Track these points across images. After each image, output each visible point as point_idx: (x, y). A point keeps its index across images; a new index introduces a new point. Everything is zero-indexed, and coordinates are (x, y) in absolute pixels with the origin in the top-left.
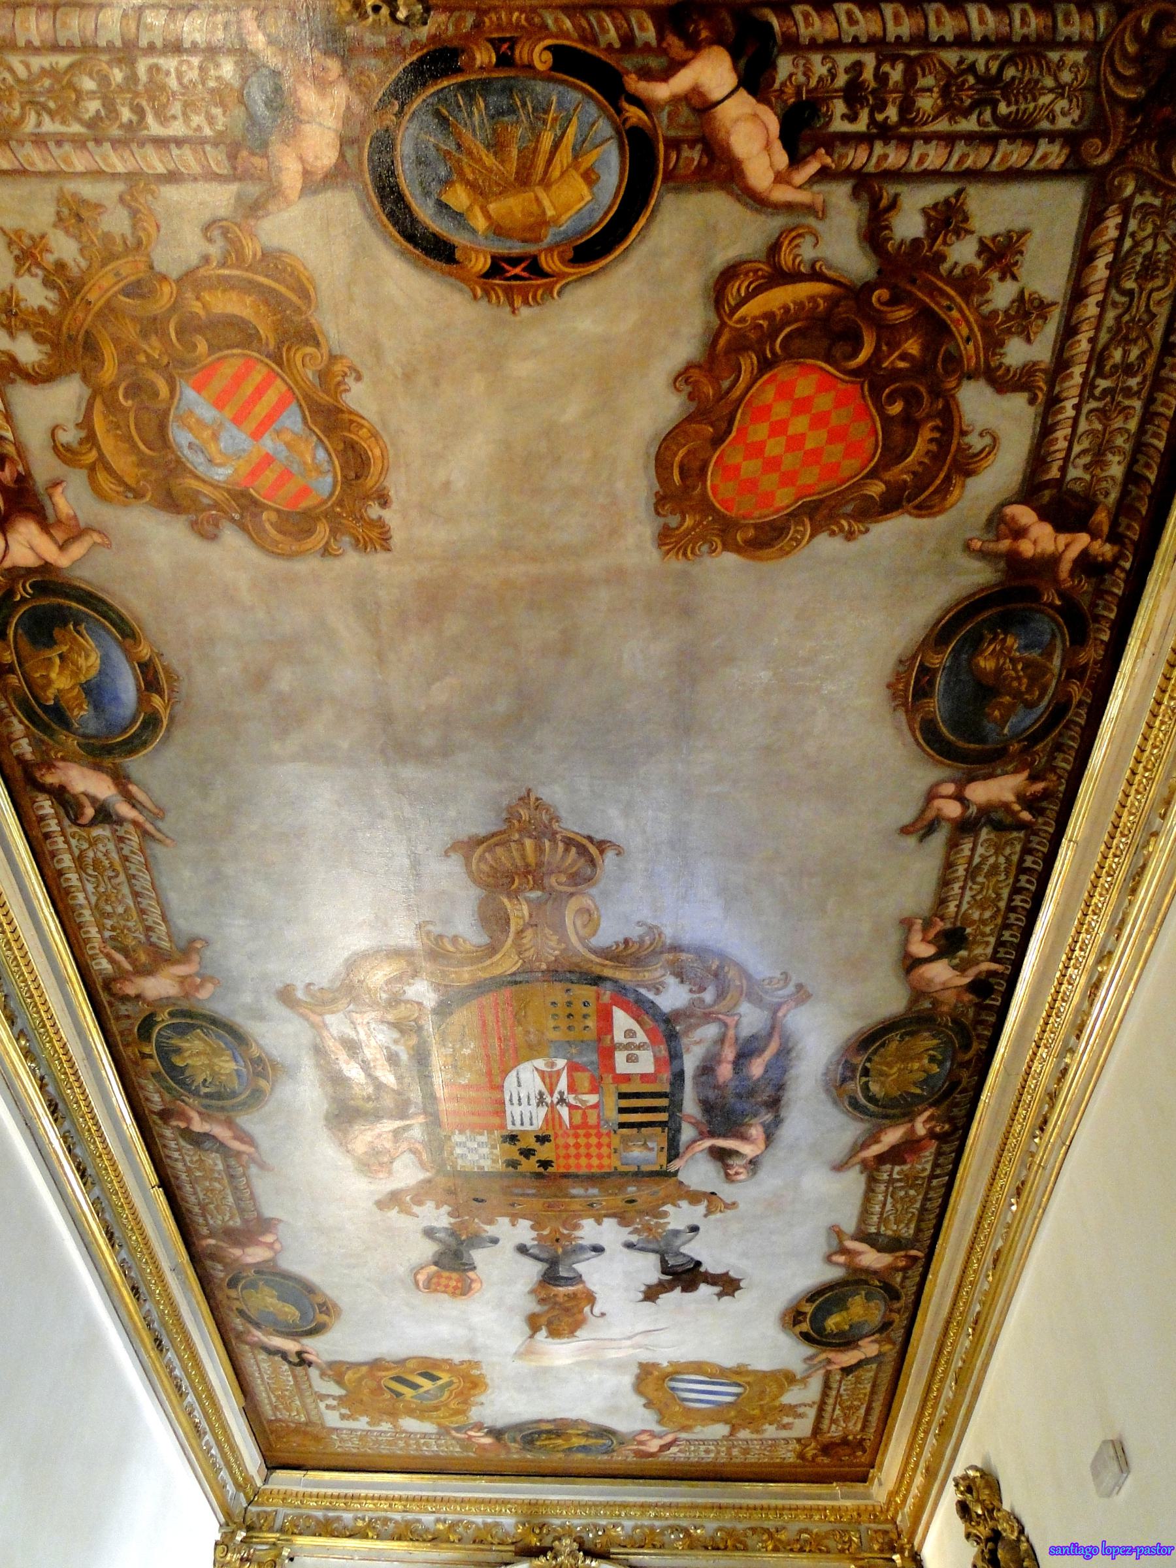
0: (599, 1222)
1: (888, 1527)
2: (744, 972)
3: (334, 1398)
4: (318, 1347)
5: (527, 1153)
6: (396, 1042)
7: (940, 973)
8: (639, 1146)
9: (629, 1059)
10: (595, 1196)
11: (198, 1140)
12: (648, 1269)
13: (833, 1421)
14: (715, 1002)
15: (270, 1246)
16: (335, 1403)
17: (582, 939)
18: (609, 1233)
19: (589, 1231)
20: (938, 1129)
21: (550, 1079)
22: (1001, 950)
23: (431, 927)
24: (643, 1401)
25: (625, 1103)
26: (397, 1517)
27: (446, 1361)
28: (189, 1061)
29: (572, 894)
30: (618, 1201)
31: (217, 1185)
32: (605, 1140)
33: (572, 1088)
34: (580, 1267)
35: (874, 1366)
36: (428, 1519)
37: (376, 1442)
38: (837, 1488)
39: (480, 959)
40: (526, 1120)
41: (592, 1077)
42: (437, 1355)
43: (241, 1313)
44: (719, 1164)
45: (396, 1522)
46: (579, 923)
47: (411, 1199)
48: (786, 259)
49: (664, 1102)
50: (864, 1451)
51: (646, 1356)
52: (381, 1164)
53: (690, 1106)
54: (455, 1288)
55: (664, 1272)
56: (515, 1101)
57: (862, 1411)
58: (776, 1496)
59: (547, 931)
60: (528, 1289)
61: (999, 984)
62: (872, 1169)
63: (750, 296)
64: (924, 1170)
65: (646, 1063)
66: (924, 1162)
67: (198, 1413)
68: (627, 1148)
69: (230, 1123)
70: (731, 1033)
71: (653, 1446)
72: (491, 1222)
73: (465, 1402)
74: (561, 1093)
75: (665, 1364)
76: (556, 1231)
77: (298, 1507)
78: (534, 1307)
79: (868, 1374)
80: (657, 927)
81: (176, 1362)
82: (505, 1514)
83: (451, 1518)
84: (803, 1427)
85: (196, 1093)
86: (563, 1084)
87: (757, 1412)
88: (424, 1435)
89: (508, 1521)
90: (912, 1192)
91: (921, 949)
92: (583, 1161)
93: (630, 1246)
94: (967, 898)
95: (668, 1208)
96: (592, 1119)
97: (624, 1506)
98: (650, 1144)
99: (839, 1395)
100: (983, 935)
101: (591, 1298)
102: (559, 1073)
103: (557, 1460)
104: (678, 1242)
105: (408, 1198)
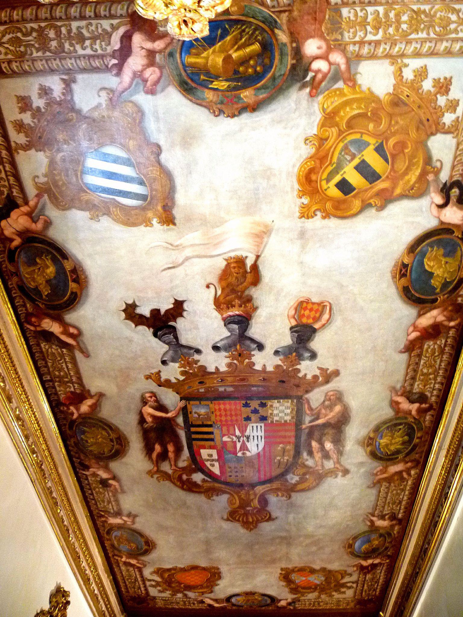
5: (255, 411)
9: (211, 455)
10: (221, 386)
21: (244, 448)
25: (211, 436)
30: (209, 383)
32: (218, 418)
40: (255, 428)
44: (161, 403)
46: (234, 501)
47: (319, 378)
49: (194, 436)
53: (182, 434)
55: (174, 329)
60: (259, 312)
68: (207, 414)
70: (173, 463)
74: (239, 441)
78: (255, 292)
86: (239, 445)
92: (228, 407)
93: (198, 351)
95: (182, 378)
96: (225, 428)
98: (196, 415)
101: (218, 304)
102: (240, 450)
105: (321, 379)
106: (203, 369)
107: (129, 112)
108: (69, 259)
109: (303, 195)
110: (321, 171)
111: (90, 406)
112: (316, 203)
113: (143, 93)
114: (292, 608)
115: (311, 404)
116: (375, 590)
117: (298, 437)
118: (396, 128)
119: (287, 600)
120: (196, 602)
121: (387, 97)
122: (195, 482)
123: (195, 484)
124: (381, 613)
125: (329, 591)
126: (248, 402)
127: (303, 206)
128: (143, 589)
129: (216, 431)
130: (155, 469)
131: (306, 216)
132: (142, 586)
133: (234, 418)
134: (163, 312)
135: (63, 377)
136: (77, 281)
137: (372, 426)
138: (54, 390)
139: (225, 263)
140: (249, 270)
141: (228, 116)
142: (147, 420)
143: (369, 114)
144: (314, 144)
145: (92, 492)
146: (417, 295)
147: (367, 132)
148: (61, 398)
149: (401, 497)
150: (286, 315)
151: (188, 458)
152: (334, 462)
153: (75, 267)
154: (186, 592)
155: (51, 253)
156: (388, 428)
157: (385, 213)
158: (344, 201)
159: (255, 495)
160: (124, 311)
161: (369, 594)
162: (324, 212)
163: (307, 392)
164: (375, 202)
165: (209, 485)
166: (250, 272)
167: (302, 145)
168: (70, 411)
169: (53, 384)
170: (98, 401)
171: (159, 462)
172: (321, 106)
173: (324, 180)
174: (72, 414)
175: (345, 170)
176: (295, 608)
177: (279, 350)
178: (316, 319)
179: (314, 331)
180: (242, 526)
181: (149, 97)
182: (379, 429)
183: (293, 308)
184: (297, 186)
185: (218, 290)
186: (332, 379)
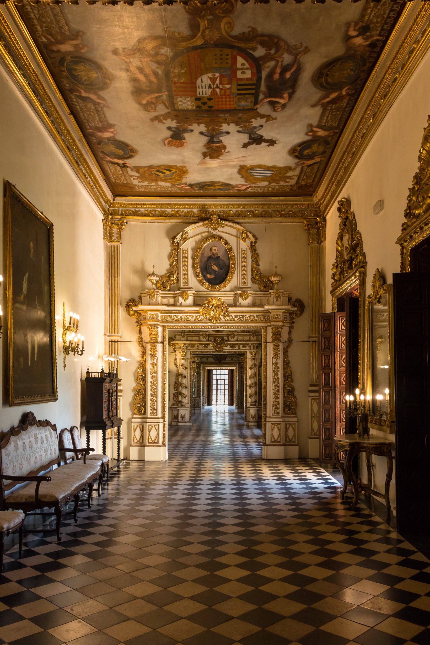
0: (229, 125)
1: (317, 209)
2: (286, 43)
3: (136, 176)
4: (130, 162)
5: (204, 104)
6: (157, 68)
7: (359, 41)
10: (228, 117)
11: (84, 99)
12: (245, 138)
13: (303, 180)
14: (275, 54)
15: (112, 132)
16: (136, 178)
17: (227, 33)
18: (232, 128)
19: (225, 127)
20: (350, 92)
21: (213, 80)
22: (383, 32)
23: (170, 29)
24: (241, 176)
26: (159, 210)
27: (175, 166)
28: (79, 73)
29: (224, 17)
31: (92, 113)
33: (221, 83)
34: (221, 138)
35: (318, 164)
36: (169, 210)
37: (151, 188)
38: (302, 198)
39: (189, 40)
40: (204, 93)
42: (171, 164)
43: (103, 152)
44: (272, 106)
45: (159, 211)
46: (226, 27)
49: (254, 87)
50: (312, 188)
51: (242, 164)
52: (152, 108)
53: (263, 88)
54: (178, 145)
56: (200, 87)
57: (313, 177)
58: (282, 201)
59: (214, 30)
60: (203, 145)
61: (380, 44)
62: (324, 107)
64: (343, 105)
65: (248, 74)
66: (344, 103)
67: (91, 183)
69: (96, 94)
70: (280, 64)
71: (243, 188)
72: (191, 125)
73: (181, 177)
74: (217, 85)
75: (249, 166)
77: (126, 207)
79: (316, 167)
80: (255, 28)
81: (83, 169)
82: (194, 208)
83: (176, 210)
84: (293, 182)
85: (83, 84)
86: (218, 82)
87: (278, 178)
88: (167, 186)
89: (195, 210)
90: (338, 113)
91: (352, 33)
93: (238, 132)
94: (373, 14)
95: (253, 120)
96: (228, 93)
97: (232, 205)
98: (248, 100)
99: (306, 173)
100: (377, 27)
101: (225, 147)
102: (216, 78)
103: (211, 192)
104: (256, 130)
105: (162, 118)
122: (263, 47)
126: (209, 109)
129: (235, 90)
151: (264, 70)
159: (203, 36)
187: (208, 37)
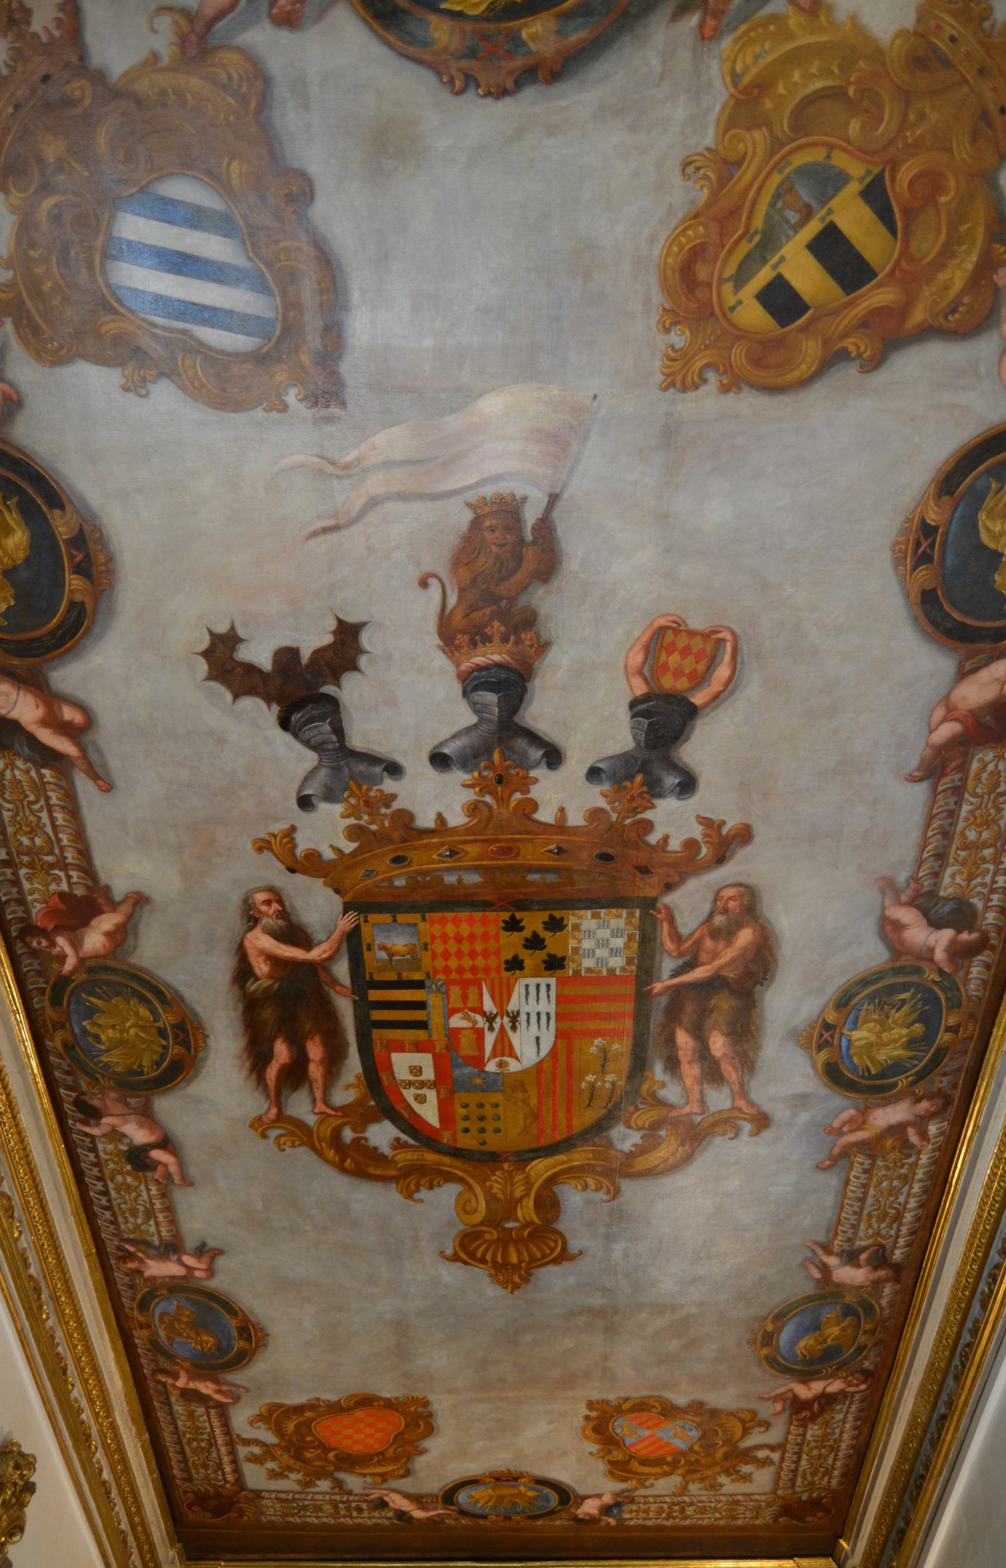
5: (535, 943)
8: (397, 953)
9: (416, 1070)
10: (448, 870)
21: (504, 1048)
25: (418, 1015)
29: (481, 1224)
32: (440, 963)
33: (480, 1034)
40: (532, 991)
41: (457, 1050)
44: (293, 919)
46: (474, 1202)
47: (699, 850)
48: (379, 1479)
49: (377, 1015)
53: (345, 1008)
55: (333, 702)
59: (500, 1196)
60: (553, 655)
63: (394, 1471)
68: (412, 950)
70: (318, 1095)
76: (503, 801)
80: (406, 1198)
86: (490, 1040)
92: (465, 930)
93: (394, 769)
95: (349, 847)
96: (455, 991)
98: (383, 955)
102: (494, 1054)
105: (704, 851)
106: (405, 817)
107: (230, 79)
108: (68, 508)
109: (672, 324)
110: (722, 255)
111: (108, 934)
112: (707, 347)
113: (267, 24)
114: (612, 1521)
115: (679, 921)
116: (828, 1472)
117: (641, 1016)
118: (919, 132)
119: (599, 1496)
120: (364, 1506)
121: (898, 42)
122: (375, 1149)
123: (374, 1155)
124: (843, 1543)
125: (708, 1473)
127: (673, 355)
128: (228, 1469)
129: (434, 1001)
130: (274, 1111)
131: (678, 384)
132: (226, 1459)
133: (480, 962)
134: (305, 655)
135: (40, 851)
136: (84, 569)
137: (832, 989)
138: (15, 890)
139: (468, 516)
140: (529, 537)
141: (488, 94)
142: (257, 971)
143: (851, 91)
144: (706, 177)
145: (105, 1186)
146: (956, 615)
147: (844, 144)
148: (34, 911)
149: (902, 1199)
150: (621, 665)
152: (732, 1091)
153: (81, 531)
154: (342, 1476)
155: (20, 490)
156: (871, 997)
157: (880, 378)
158: (779, 343)
159: (528, 1183)
160: (206, 654)
161: (812, 1483)
162: (725, 372)
163: (669, 887)
164: (858, 348)
165: (409, 1156)
166: (534, 543)
167: (678, 180)
168: (58, 949)
169: (15, 874)
170: (130, 917)
171: (285, 1092)
172: (727, 66)
173: (730, 279)
174: (62, 958)
175: (782, 252)
176: (620, 1521)
177: (600, 765)
178: (699, 680)
179: (692, 712)
180: (490, 1276)
181: (284, 35)
182: (850, 999)
183: (638, 647)
184: (657, 298)
185: (449, 592)
186: (733, 853)
187: (516, 1179)
